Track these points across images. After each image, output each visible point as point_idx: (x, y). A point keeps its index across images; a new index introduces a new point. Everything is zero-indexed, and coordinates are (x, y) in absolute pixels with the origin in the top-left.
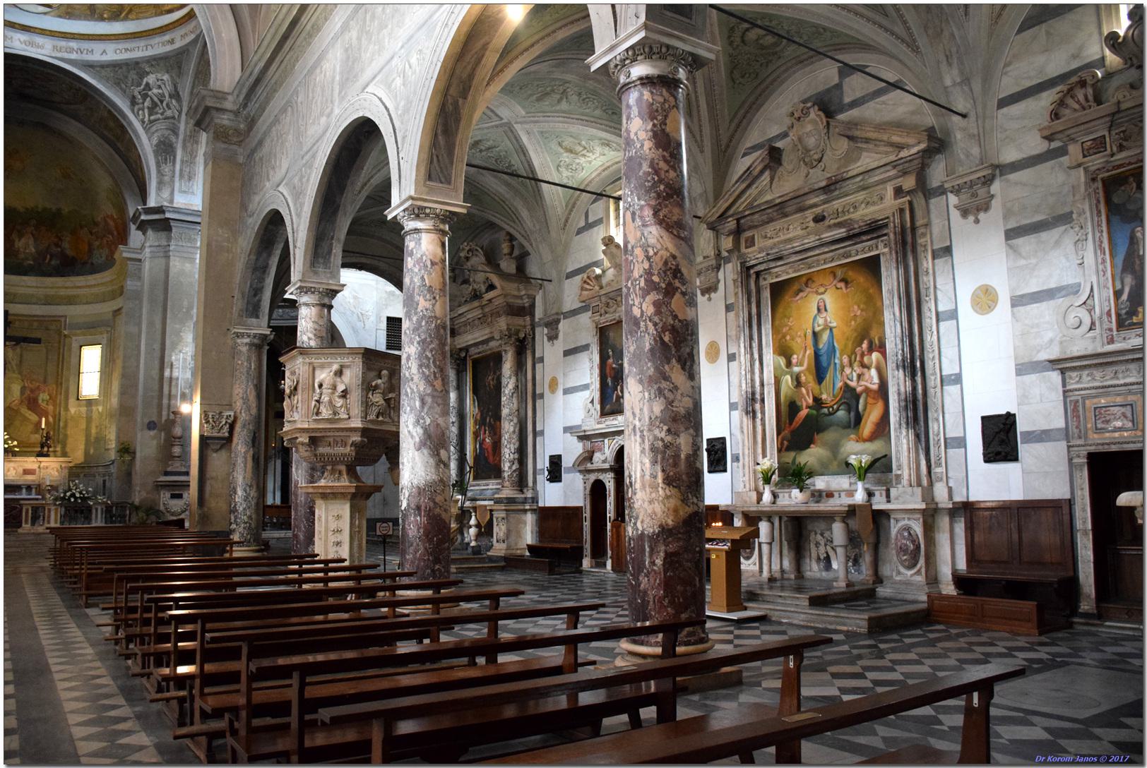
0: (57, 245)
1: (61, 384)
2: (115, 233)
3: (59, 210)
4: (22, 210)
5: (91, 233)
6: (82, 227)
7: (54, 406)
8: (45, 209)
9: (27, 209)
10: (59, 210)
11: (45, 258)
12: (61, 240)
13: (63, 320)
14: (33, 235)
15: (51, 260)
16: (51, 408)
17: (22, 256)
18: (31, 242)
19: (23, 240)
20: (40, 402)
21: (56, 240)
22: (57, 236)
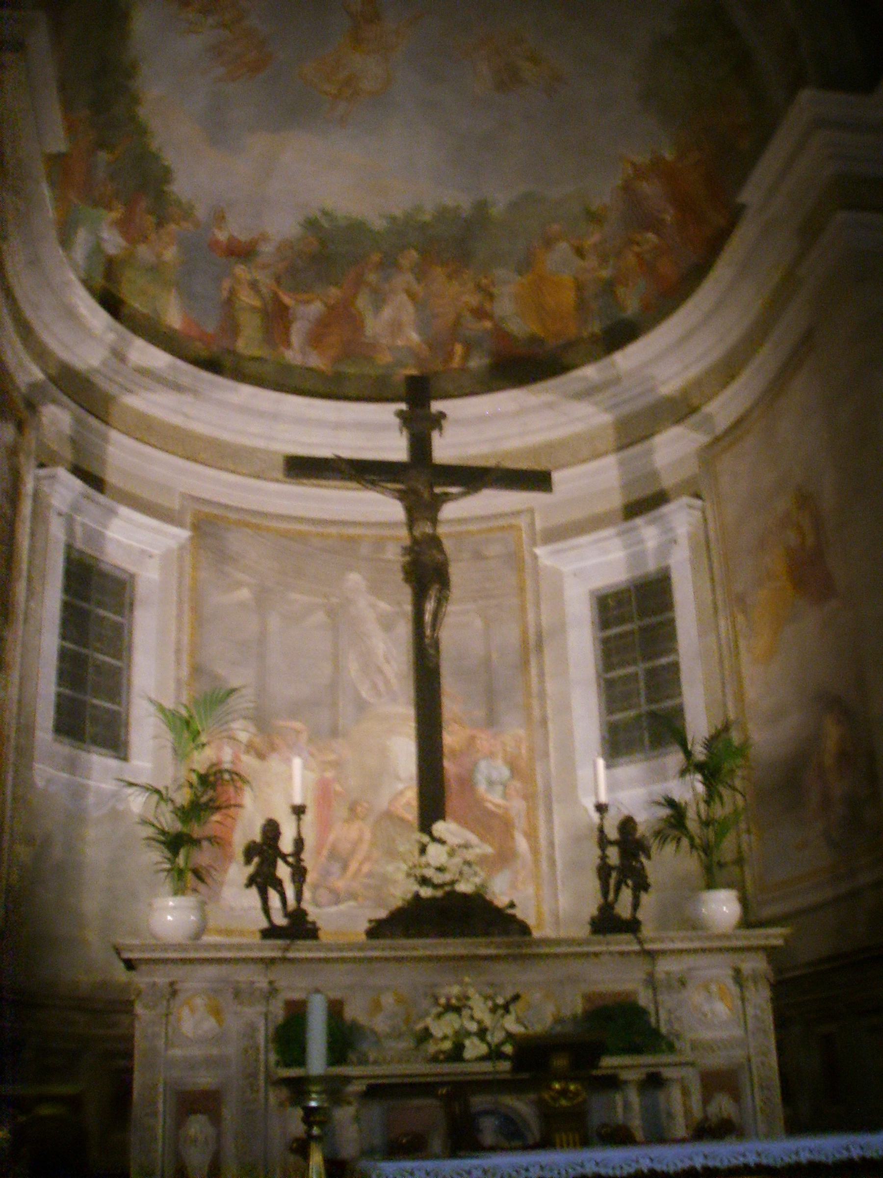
0: (480, 313)
1: (544, 722)
2: (669, 216)
3: (482, 206)
4: (379, 224)
5: (580, 252)
6: (549, 243)
7: (529, 797)
8: (443, 214)
9: (394, 219)
10: (482, 206)
11: (450, 355)
12: (491, 297)
13: (522, 522)
14: (412, 296)
15: (466, 356)
16: (517, 806)
17: (385, 358)
18: (408, 313)
19: (387, 313)
20: (482, 788)
21: (473, 300)
22: (479, 288)
